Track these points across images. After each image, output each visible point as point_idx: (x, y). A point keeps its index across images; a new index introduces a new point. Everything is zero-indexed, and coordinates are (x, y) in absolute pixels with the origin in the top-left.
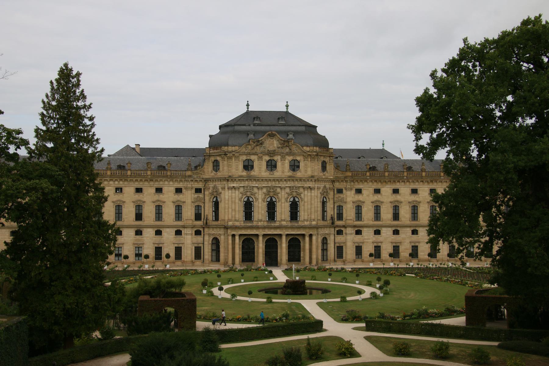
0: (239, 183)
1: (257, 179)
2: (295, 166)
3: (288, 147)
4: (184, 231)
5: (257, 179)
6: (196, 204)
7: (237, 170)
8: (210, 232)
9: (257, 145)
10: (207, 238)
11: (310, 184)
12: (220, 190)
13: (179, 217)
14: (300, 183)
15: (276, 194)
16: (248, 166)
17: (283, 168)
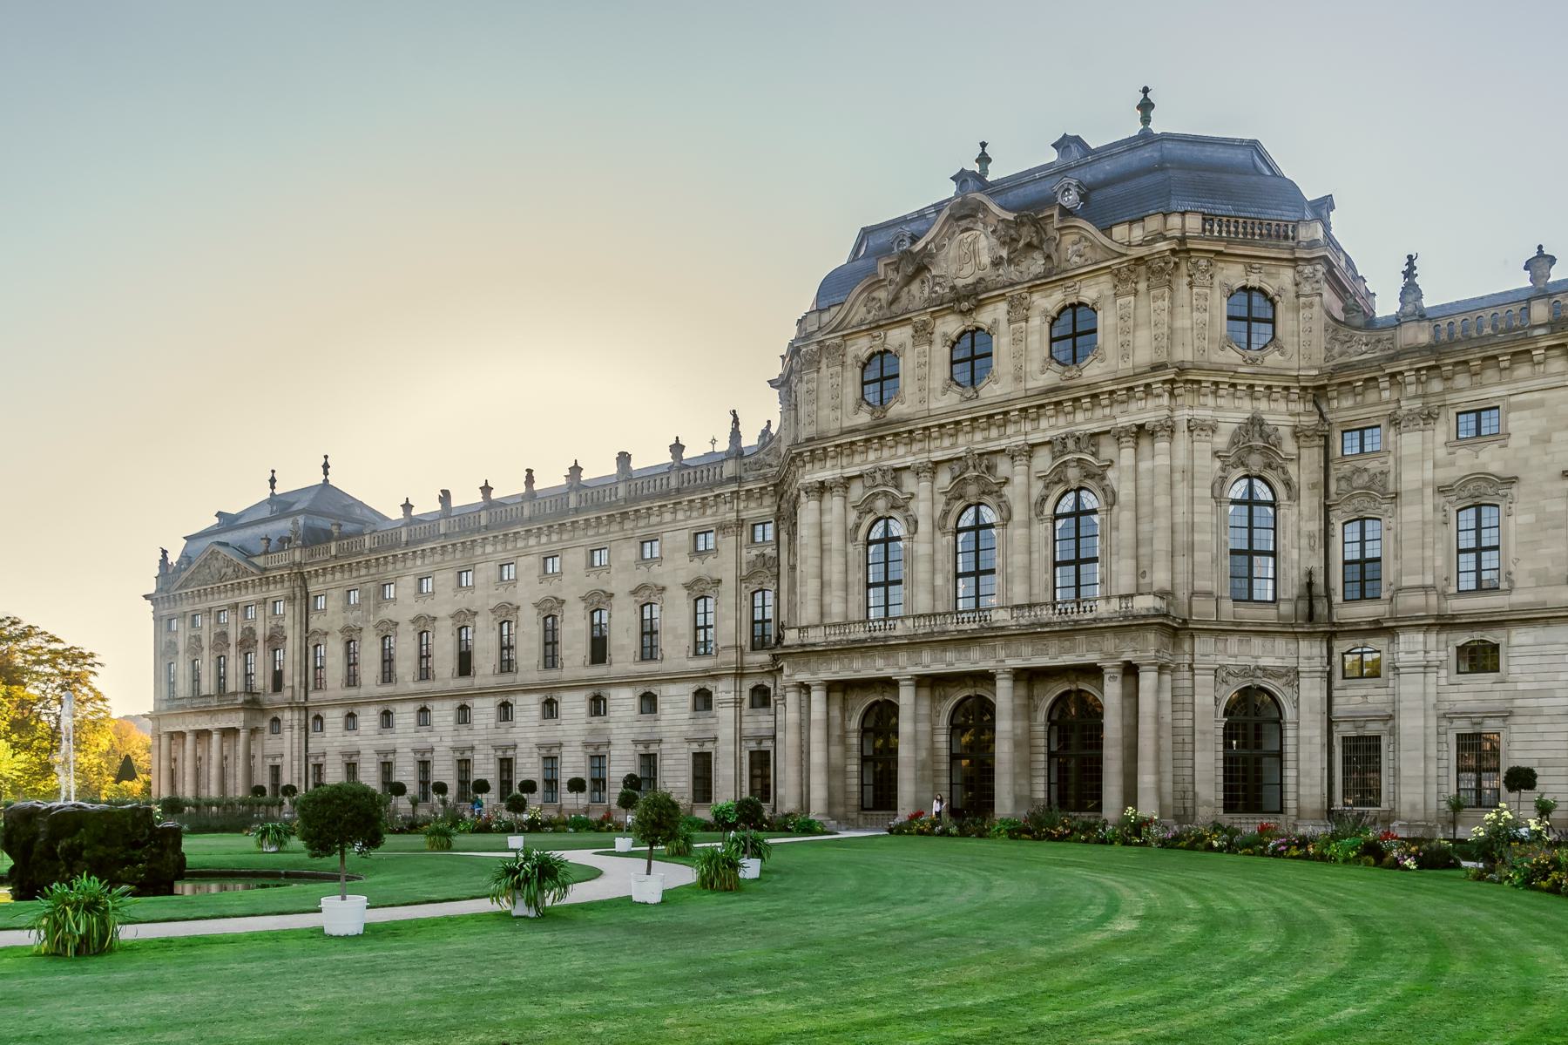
1: (906, 433)
5: (906, 433)
7: (834, 408)
11: (1146, 411)
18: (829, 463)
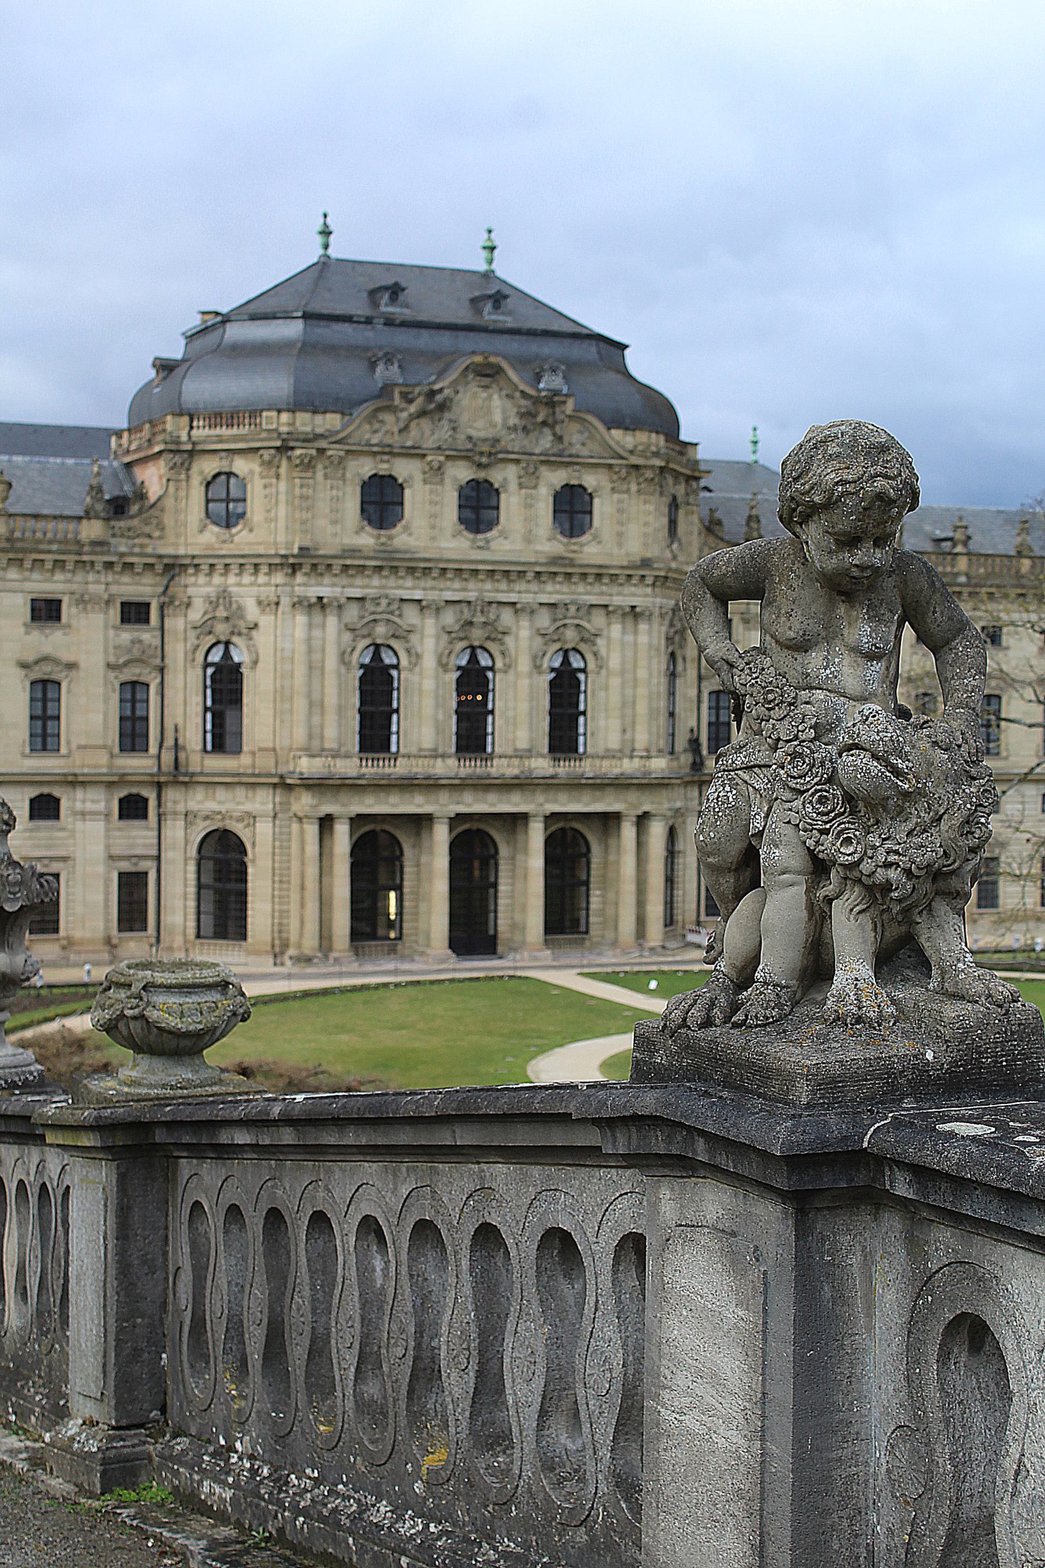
0: (345, 581)
2: (572, 509)
3: (552, 427)
4: (69, 801)
5: (418, 568)
6: (128, 675)
7: (335, 522)
8: (193, 806)
9: (422, 414)
10: (175, 831)
12: (252, 612)
13: (44, 735)
14: (597, 588)
15: (497, 634)
16: (382, 501)
17: (525, 521)
18: (327, 580)
